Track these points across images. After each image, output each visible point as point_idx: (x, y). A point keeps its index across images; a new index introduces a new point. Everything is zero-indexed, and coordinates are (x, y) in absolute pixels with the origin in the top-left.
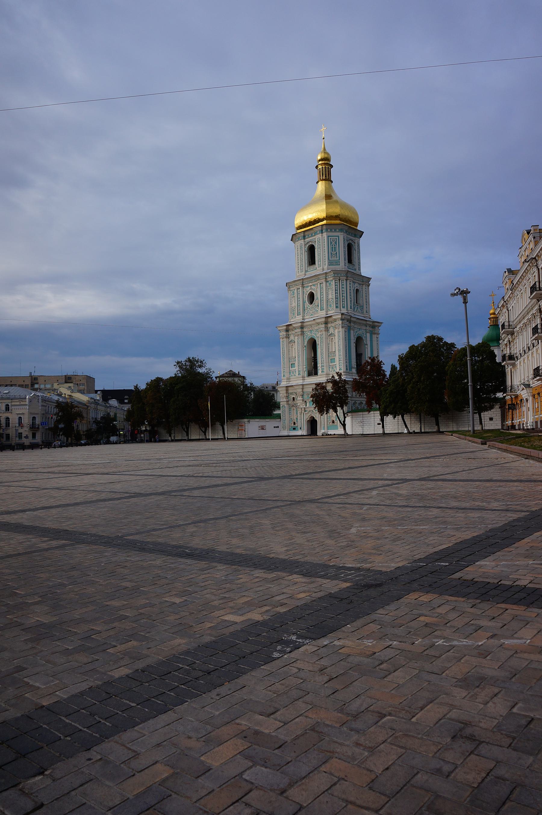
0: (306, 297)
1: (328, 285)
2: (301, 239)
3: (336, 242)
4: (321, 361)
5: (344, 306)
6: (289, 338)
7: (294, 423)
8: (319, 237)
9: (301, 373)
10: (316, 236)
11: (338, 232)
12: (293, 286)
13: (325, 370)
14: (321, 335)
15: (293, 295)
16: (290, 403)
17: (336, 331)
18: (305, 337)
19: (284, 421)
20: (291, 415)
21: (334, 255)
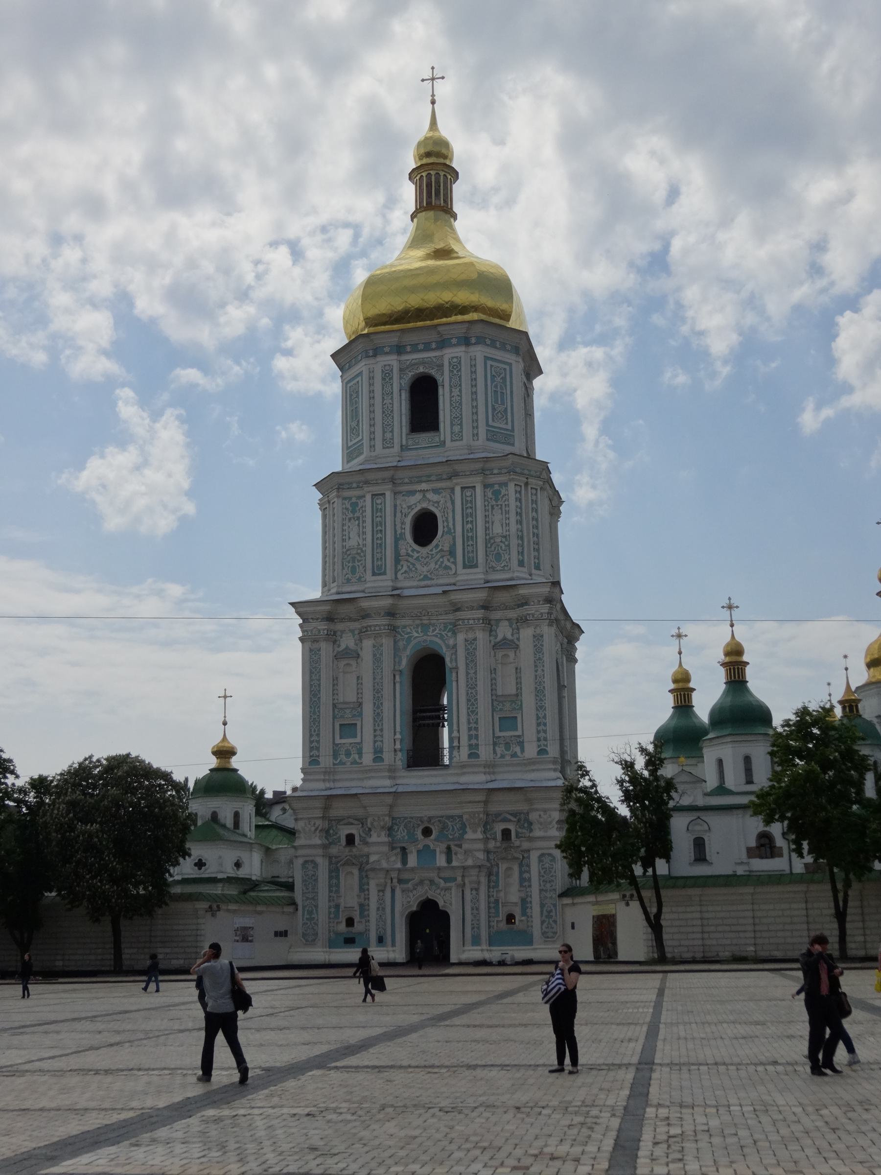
0: (403, 523)
1: (490, 494)
2: (387, 353)
3: (504, 379)
4: (469, 723)
5: (539, 563)
7: (350, 922)
8: (459, 355)
12: (354, 485)
14: (471, 643)
15: (353, 512)
16: (334, 850)
17: (526, 634)
19: (310, 913)
20: (337, 892)
21: (499, 414)
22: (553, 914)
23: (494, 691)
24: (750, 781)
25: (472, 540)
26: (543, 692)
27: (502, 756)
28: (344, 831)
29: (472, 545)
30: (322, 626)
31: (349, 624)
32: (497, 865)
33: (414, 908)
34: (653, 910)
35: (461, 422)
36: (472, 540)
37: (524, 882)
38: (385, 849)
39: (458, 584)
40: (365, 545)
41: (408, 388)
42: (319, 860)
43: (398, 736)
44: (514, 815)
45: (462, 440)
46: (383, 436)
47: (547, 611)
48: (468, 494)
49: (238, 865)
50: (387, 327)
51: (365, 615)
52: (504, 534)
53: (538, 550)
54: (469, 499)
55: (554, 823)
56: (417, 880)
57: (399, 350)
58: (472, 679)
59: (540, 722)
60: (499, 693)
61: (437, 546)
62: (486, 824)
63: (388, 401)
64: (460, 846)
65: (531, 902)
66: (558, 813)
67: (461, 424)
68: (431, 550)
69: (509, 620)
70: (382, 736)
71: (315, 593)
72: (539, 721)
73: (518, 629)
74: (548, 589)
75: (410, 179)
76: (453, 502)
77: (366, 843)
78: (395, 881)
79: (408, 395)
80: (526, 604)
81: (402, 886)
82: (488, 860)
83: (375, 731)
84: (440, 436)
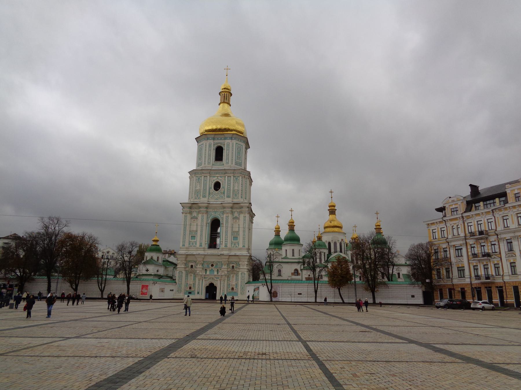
0: (211, 184)
3: (240, 149)
4: (225, 238)
6: (191, 214)
7: (190, 288)
8: (229, 142)
9: (203, 245)
10: (226, 141)
11: (242, 142)
13: (228, 245)
15: (199, 180)
16: (187, 269)
17: (242, 216)
18: (209, 216)
19: (180, 285)
20: (187, 280)
22: (244, 288)
24: (293, 256)
27: (233, 247)
28: (190, 264)
30: (188, 210)
31: (195, 210)
32: (230, 275)
33: (208, 285)
34: (270, 288)
37: (237, 280)
38: (201, 269)
40: (201, 189)
41: (215, 149)
42: (183, 271)
43: (206, 240)
44: (235, 262)
46: (208, 161)
48: (229, 178)
49: (158, 271)
50: (211, 133)
51: (200, 207)
53: (246, 194)
54: (229, 179)
55: (246, 265)
56: (209, 278)
57: (214, 139)
59: (244, 239)
60: (234, 230)
62: (227, 265)
63: (210, 152)
64: (221, 270)
65: (238, 285)
66: (247, 262)
67: (229, 160)
69: (238, 212)
70: (202, 240)
71: (186, 200)
73: (240, 214)
75: (219, 94)
76: (225, 180)
77: (196, 268)
78: (203, 278)
79: (215, 151)
80: (242, 208)
81: (205, 279)
82: (228, 273)
83: (200, 238)
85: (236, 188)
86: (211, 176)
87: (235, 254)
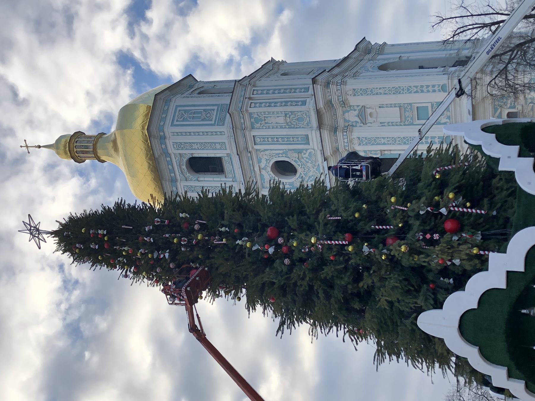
1: (258, 125)
3: (186, 111)
5: (305, 88)
8: (172, 144)
10: (170, 152)
17: (353, 101)
21: (208, 115)
23: (398, 124)
25: (290, 138)
26: (397, 88)
27: (449, 118)
29: (293, 138)
35: (213, 143)
36: (290, 138)
39: (321, 149)
45: (224, 143)
47: (335, 86)
52: (284, 115)
53: (296, 89)
54: (262, 140)
57: (174, 181)
58: (389, 141)
59: (420, 90)
61: (295, 161)
67: (215, 143)
68: (299, 165)
72: (420, 91)
73: (350, 106)
74: (319, 86)
76: (267, 150)
80: (330, 101)
84: (224, 157)
85: (281, 120)
86: (262, 183)
87: (469, 114)
